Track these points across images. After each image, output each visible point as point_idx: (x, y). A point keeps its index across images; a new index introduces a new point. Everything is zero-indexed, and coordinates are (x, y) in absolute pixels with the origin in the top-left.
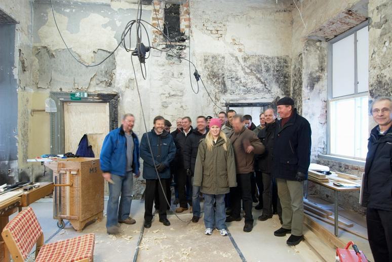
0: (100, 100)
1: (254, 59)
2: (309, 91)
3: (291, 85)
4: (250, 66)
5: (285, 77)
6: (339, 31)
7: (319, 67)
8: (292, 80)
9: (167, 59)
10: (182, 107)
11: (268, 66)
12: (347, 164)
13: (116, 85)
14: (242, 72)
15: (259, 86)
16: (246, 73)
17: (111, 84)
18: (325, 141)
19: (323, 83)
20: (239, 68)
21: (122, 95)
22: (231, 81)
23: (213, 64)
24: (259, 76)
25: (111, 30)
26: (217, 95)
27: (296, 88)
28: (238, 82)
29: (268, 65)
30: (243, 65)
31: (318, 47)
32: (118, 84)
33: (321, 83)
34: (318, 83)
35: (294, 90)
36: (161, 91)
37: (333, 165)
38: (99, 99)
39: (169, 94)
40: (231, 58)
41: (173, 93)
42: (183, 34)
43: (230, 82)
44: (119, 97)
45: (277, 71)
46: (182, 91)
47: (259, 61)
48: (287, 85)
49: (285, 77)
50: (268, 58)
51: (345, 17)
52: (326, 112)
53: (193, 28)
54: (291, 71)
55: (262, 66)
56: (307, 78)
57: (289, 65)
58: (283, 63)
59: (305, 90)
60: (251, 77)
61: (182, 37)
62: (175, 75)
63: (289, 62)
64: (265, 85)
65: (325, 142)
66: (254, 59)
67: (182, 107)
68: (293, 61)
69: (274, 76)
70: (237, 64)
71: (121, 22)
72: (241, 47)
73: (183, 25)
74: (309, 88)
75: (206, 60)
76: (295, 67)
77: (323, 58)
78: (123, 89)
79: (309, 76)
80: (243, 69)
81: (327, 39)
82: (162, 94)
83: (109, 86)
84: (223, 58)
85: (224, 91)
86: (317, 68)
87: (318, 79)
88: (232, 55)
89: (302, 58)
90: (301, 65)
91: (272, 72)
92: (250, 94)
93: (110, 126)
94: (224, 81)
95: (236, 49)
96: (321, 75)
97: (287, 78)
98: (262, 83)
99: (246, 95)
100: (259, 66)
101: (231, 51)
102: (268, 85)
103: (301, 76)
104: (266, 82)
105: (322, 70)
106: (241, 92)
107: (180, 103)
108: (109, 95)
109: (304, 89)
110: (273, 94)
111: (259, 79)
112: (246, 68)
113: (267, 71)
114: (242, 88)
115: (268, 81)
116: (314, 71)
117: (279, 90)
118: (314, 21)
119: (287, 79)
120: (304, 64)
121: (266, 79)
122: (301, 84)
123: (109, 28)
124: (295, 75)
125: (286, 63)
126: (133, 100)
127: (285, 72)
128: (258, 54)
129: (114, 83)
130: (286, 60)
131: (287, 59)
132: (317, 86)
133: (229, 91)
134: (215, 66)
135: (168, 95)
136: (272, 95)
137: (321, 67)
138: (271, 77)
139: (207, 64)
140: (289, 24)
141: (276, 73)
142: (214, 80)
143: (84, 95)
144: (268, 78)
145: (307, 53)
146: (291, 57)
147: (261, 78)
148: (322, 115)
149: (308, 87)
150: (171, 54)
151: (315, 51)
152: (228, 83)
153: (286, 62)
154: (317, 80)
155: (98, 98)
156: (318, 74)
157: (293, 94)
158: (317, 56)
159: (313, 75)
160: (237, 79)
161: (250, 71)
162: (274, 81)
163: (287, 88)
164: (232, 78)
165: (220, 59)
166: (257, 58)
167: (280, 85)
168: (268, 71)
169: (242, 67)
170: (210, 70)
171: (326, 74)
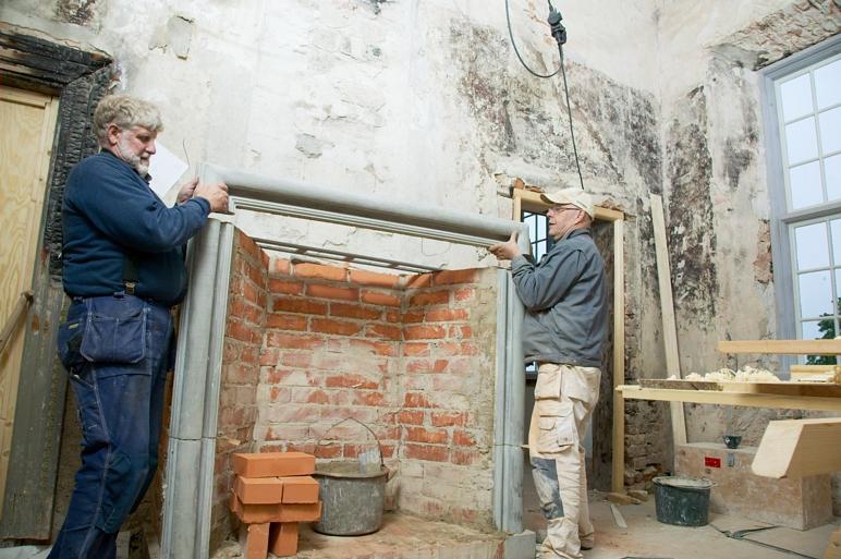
1: (583, 77)
2: (729, 188)
3: (664, 174)
5: (651, 149)
7: (744, 129)
10: (371, 168)
11: (615, 105)
13: (109, 23)
15: (596, 155)
17: (89, 13)
21: (131, 73)
22: (527, 119)
23: (476, 51)
24: (595, 127)
26: (488, 154)
27: (685, 180)
29: (613, 102)
32: (121, 22)
33: (751, 168)
34: (745, 169)
38: (15, 63)
39: (327, 109)
41: (339, 109)
44: (113, 77)
45: (634, 127)
46: (375, 111)
47: (592, 80)
48: (655, 170)
49: (651, 149)
54: (662, 135)
57: (657, 119)
59: (718, 184)
62: (357, 51)
63: (655, 112)
64: (610, 157)
66: (583, 77)
67: (371, 168)
69: (627, 137)
74: (728, 179)
75: (456, 35)
76: (677, 123)
77: (750, 110)
78: (140, 48)
82: (299, 104)
83: (72, 19)
86: (741, 132)
87: (746, 159)
89: (704, 98)
90: (703, 118)
94: (508, 116)
96: (750, 150)
97: (655, 152)
98: (605, 150)
103: (701, 145)
104: (610, 148)
105: (752, 137)
107: (367, 153)
111: (595, 136)
114: (556, 150)
115: (617, 148)
116: (735, 136)
117: (640, 180)
120: (711, 114)
121: (612, 142)
122: (705, 167)
124: (678, 145)
129: (103, 14)
130: (649, 105)
132: (744, 177)
134: (481, 61)
136: (626, 192)
137: (750, 130)
138: (622, 138)
139: (458, 46)
141: (630, 131)
144: (616, 138)
145: (716, 89)
146: (658, 99)
147: (600, 136)
151: (733, 88)
153: (649, 108)
154: (742, 161)
155: (9, 53)
156: (744, 147)
158: (738, 102)
159: (734, 147)
160: (542, 119)
163: (656, 178)
164: (528, 109)
165: (495, 44)
166: (588, 76)
167: (640, 165)
168: (613, 118)
169: (553, 86)
171: (762, 150)
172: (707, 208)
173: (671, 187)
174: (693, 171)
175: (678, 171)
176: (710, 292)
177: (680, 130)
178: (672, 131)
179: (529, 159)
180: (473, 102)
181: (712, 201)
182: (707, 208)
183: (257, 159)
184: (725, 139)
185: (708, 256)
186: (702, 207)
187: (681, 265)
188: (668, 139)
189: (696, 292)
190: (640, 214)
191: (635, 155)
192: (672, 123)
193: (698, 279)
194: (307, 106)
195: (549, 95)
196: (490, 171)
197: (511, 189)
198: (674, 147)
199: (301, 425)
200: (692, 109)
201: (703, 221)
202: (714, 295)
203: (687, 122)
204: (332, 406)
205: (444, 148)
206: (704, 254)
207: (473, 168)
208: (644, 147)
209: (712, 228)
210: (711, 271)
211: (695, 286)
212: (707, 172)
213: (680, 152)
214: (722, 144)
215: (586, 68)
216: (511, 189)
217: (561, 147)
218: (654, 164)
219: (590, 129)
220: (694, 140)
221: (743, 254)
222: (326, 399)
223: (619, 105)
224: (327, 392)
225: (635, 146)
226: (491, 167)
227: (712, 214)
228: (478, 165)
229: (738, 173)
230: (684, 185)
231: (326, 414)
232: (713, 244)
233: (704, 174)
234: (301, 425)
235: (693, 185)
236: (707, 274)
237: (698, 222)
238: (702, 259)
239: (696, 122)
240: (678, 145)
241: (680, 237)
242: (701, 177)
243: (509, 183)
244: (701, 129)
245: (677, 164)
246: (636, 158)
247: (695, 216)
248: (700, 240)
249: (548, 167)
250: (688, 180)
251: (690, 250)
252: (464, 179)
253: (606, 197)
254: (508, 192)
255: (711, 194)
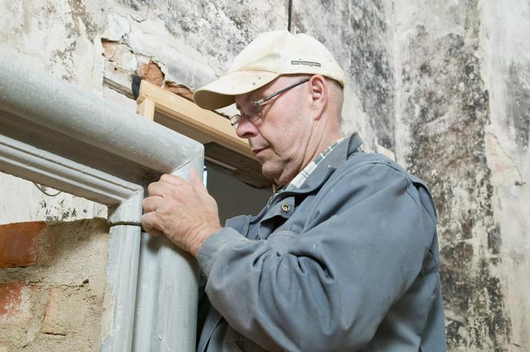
2: (514, 146)
3: (398, 116)
27: (436, 127)
56: (503, 87)
57: (388, 22)
63: (385, 10)
74: (513, 131)
76: (422, 32)
79: (507, 76)
97: (385, 78)
103: (469, 70)
120: (487, 19)
122: (475, 107)
125: (379, 8)
141: (350, 31)
149: (508, 123)
163: (386, 122)
167: (364, 93)
172: (479, 177)
173: (409, 140)
174: (452, 112)
175: (424, 112)
176: (492, 333)
177: (429, 43)
178: (413, 45)
179: (177, 28)
181: (491, 163)
182: (479, 177)
184: (508, 63)
185: (483, 264)
186: (469, 175)
188: (407, 58)
189: (462, 331)
192: (413, 32)
193: (464, 306)
196: (91, 29)
197: (136, 81)
198: (416, 72)
200: (452, 10)
201: (471, 199)
202: (500, 338)
203: (440, 29)
206: (476, 259)
208: (369, 64)
209: (489, 213)
210: (492, 292)
211: (460, 318)
212: (479, 114)
213: (428, 81)
216: (136, 81)
217: (239, 24)
218: (384, 98)
220: (453, 60)
225: (356, 58)
226: (96, 19)
227: (489, 187)
230: (436, 136)
232: (493, 241)
233: (474, 118)
235: (452, 137)
236: (485, 297)
237: (461, 201)
238: (473, 269)
239: (459, 30)
240: (424, 69)
242: (467, 123)
243: (132, 64)
244: (468, 41)
245: (422, 101)
246: (358, 81)
247: (456, 191)
248: (467, 232)
249: (212, 53)
250: (443, 128)
252: (26, 26)
254: (128, 85)
255: (487, 154)
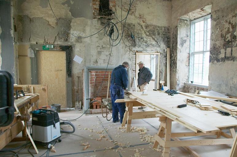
0: (61, 50)
3: (171, 43)
4: (149, 31)
6: (196, 17)
8: (171, 41)
9: (101, 25)
12: (199, 87)
13: (70, 40)
14: (145, 34)
15: (154, 43)
16: (147, 35)
17: (67, 39)
18: (188, 75)
19: (187, 43)
20: (143, 32)
21: (74, 47)
22: (139, 39)
24: (154, 37)
25: (68, 6)
27: (174, 45)
28: (142, 40)
30: (145, 30)
31: (186, 23)
32: (72, 40)
35: (173, 46)
36: (97, 45)
37: (192, 88)
39: (102, 46)
40: (139, 26)
42: (111, 11)
43: (138, 40)
44: (72, 48)
45: (164, 35)
47: (154, 28)
49: (168, 38)
50: (159, 27)
51: (200, 11)
52: (189, 59)
53: (117, 8)
55: (156, 31)
57: (170, 31)
58: (168, 30)
59: (179, 46)
60: (149, 37)
61: (110, 12)
64: (157, 43)
65: (188, 76)
68: (172, 30)
69: (162, 37)
70: (142, 30)
71: (73, 2)
72: (144, 20)
73: (111, 5)
76: (173, 33)
78: (74, 43)
80: (145, 33)
81: (190, 20)
82: (98, 46)
83: (66, 41)
84: (134, 25)
85: (135, 45)
86: (185, 35)
87: (185, 41)
88: (139, 24)
89: (177, 29)
91: (161, 35)
92: (149, 48)
93: (67, 66)
95: (142, 21)
98: (156, 41)
99: (147, 48)
100: (154, 31)
101: (139, 21)
102: (158, 42)
103: (176, 39)
104: (157, 40)
105: (187, 36)
106: (144, 46)
108: (66, 46)
109: (178, 46)
110: (161, 48)
111: (154, 39)
112: (147, 32)
113: (158, 34)
117: (165, 46)
118: (185, 10)
119: (169, 40)
122: (177, 43)
123: (66, 5)
124: (173, 37)
126: (80, 50)
127: (168, 35)
128: (153, 24)
129: (69, 39)
131: (169, 28)
133: (137, 46)
135: (101, 47)
137: (187, 35)
138: (161, 38)
140: (170, 9)
142: (129, 39)
143: (51, 47)
145: (180, 27)
147: (155, 39)
148: (187, 61)
150: (104, 22)
151: (184, 26)
152: (137, 40)
153: (168, 30)
156: (185, 39)
157: (172, 48)
160: (142, 38)
161: (149, 34)
162: (162, 41)
163: (169, 45)
165: (132, 26)
166: (153, 27)
167: (165, 43)
168: (159, 34)
169: (144, 31)
170: (126, 32)
177: (174, 34)
180: (128, 39)
183: (92, 56)
187: (172, 62)
190: (164, 53)
191: (163, 41)
194: (99, 46)
195: (144, 33)
197: (135, 53)
199: (101, 93)
204: (105, 90)
205: (122, 48)
207: (128, 51)
214: (180, 38)
215: (152, 25)
219: (153, 38)
221: (183, 60)
222: (104, 90)
223: (160, 31)
224: (104, 88)
225: (164, 39)
228: (129, 50)
229: (183, 44)
231: (104, 92)
234: (101, 93)
237: (175, 54)
241: (173, 56)
251: (174, 59)
253: (156, 51)
